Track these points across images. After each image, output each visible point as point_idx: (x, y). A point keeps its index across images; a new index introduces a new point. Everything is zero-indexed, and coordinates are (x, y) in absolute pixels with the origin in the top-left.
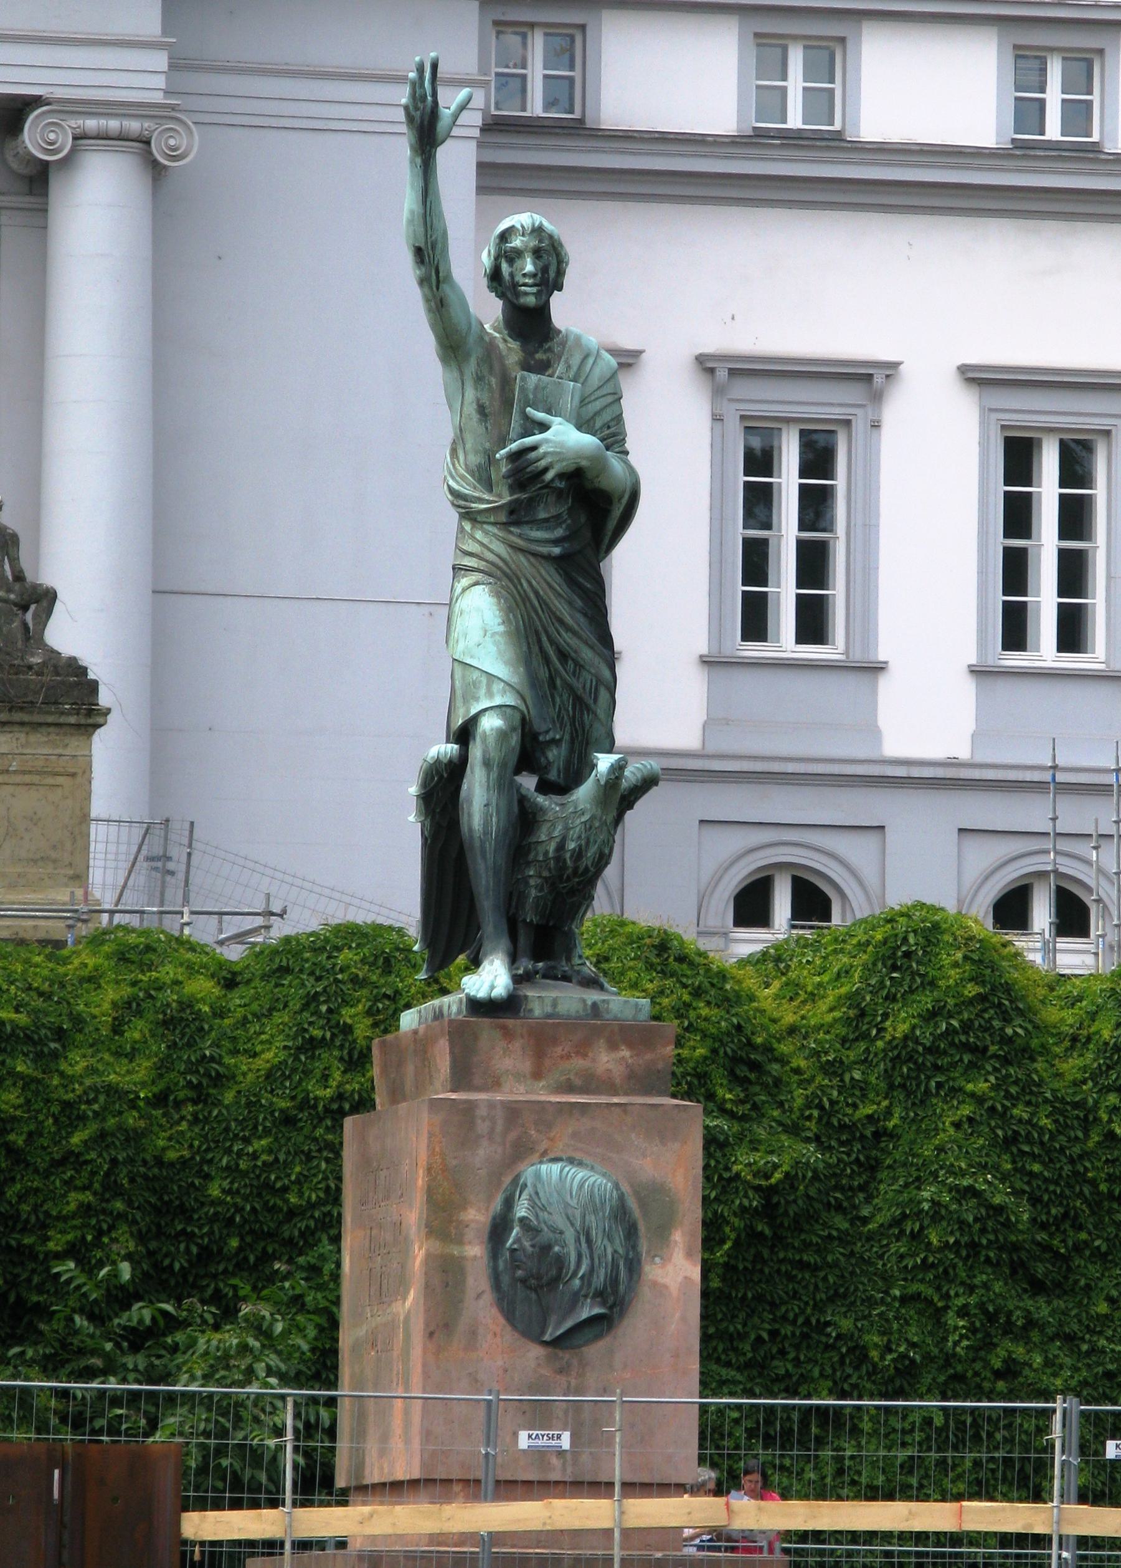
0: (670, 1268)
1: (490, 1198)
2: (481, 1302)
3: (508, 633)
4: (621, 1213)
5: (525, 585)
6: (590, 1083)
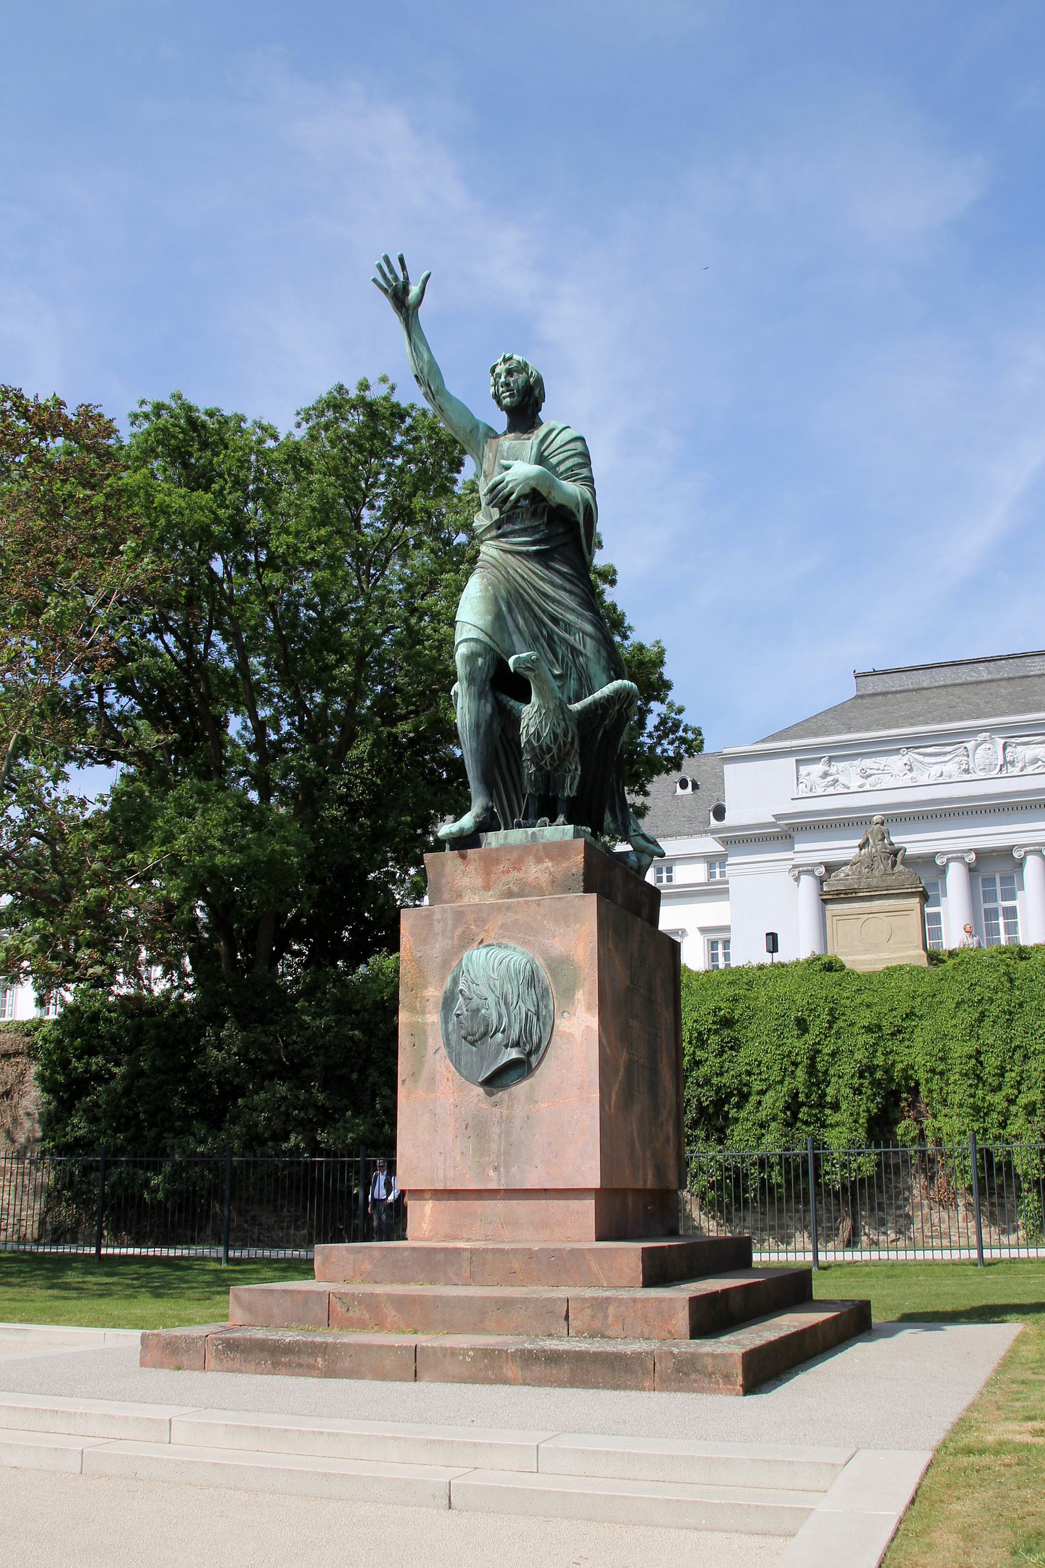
0: (575, 1020)
1: (443, 979)
2: (438, 1055)
3: (484, 597)
4: (532, 981)
5: (511, 572)
6: (523, 890)
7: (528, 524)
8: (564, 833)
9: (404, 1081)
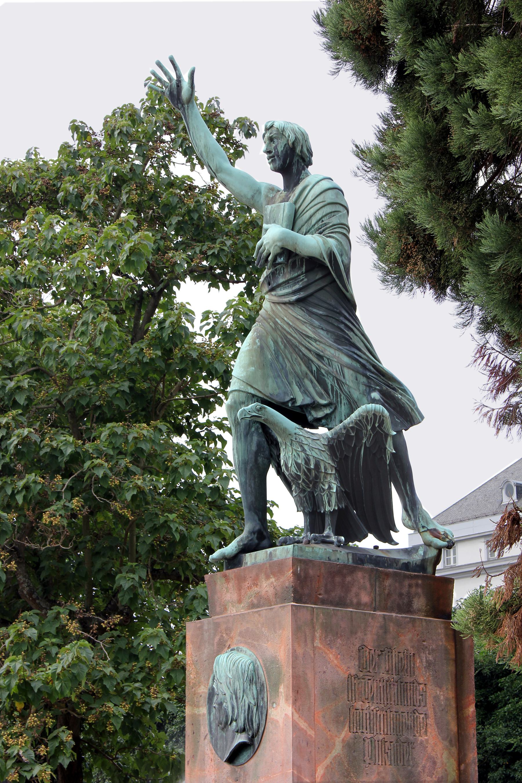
0: (279, 709)
2: (206, 741)
5: (279, 322)
7: (288, 277)
8: (287, 551)
9: (188, 762)
